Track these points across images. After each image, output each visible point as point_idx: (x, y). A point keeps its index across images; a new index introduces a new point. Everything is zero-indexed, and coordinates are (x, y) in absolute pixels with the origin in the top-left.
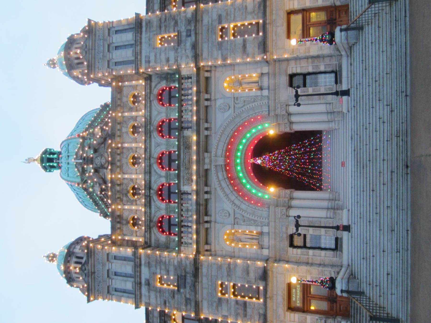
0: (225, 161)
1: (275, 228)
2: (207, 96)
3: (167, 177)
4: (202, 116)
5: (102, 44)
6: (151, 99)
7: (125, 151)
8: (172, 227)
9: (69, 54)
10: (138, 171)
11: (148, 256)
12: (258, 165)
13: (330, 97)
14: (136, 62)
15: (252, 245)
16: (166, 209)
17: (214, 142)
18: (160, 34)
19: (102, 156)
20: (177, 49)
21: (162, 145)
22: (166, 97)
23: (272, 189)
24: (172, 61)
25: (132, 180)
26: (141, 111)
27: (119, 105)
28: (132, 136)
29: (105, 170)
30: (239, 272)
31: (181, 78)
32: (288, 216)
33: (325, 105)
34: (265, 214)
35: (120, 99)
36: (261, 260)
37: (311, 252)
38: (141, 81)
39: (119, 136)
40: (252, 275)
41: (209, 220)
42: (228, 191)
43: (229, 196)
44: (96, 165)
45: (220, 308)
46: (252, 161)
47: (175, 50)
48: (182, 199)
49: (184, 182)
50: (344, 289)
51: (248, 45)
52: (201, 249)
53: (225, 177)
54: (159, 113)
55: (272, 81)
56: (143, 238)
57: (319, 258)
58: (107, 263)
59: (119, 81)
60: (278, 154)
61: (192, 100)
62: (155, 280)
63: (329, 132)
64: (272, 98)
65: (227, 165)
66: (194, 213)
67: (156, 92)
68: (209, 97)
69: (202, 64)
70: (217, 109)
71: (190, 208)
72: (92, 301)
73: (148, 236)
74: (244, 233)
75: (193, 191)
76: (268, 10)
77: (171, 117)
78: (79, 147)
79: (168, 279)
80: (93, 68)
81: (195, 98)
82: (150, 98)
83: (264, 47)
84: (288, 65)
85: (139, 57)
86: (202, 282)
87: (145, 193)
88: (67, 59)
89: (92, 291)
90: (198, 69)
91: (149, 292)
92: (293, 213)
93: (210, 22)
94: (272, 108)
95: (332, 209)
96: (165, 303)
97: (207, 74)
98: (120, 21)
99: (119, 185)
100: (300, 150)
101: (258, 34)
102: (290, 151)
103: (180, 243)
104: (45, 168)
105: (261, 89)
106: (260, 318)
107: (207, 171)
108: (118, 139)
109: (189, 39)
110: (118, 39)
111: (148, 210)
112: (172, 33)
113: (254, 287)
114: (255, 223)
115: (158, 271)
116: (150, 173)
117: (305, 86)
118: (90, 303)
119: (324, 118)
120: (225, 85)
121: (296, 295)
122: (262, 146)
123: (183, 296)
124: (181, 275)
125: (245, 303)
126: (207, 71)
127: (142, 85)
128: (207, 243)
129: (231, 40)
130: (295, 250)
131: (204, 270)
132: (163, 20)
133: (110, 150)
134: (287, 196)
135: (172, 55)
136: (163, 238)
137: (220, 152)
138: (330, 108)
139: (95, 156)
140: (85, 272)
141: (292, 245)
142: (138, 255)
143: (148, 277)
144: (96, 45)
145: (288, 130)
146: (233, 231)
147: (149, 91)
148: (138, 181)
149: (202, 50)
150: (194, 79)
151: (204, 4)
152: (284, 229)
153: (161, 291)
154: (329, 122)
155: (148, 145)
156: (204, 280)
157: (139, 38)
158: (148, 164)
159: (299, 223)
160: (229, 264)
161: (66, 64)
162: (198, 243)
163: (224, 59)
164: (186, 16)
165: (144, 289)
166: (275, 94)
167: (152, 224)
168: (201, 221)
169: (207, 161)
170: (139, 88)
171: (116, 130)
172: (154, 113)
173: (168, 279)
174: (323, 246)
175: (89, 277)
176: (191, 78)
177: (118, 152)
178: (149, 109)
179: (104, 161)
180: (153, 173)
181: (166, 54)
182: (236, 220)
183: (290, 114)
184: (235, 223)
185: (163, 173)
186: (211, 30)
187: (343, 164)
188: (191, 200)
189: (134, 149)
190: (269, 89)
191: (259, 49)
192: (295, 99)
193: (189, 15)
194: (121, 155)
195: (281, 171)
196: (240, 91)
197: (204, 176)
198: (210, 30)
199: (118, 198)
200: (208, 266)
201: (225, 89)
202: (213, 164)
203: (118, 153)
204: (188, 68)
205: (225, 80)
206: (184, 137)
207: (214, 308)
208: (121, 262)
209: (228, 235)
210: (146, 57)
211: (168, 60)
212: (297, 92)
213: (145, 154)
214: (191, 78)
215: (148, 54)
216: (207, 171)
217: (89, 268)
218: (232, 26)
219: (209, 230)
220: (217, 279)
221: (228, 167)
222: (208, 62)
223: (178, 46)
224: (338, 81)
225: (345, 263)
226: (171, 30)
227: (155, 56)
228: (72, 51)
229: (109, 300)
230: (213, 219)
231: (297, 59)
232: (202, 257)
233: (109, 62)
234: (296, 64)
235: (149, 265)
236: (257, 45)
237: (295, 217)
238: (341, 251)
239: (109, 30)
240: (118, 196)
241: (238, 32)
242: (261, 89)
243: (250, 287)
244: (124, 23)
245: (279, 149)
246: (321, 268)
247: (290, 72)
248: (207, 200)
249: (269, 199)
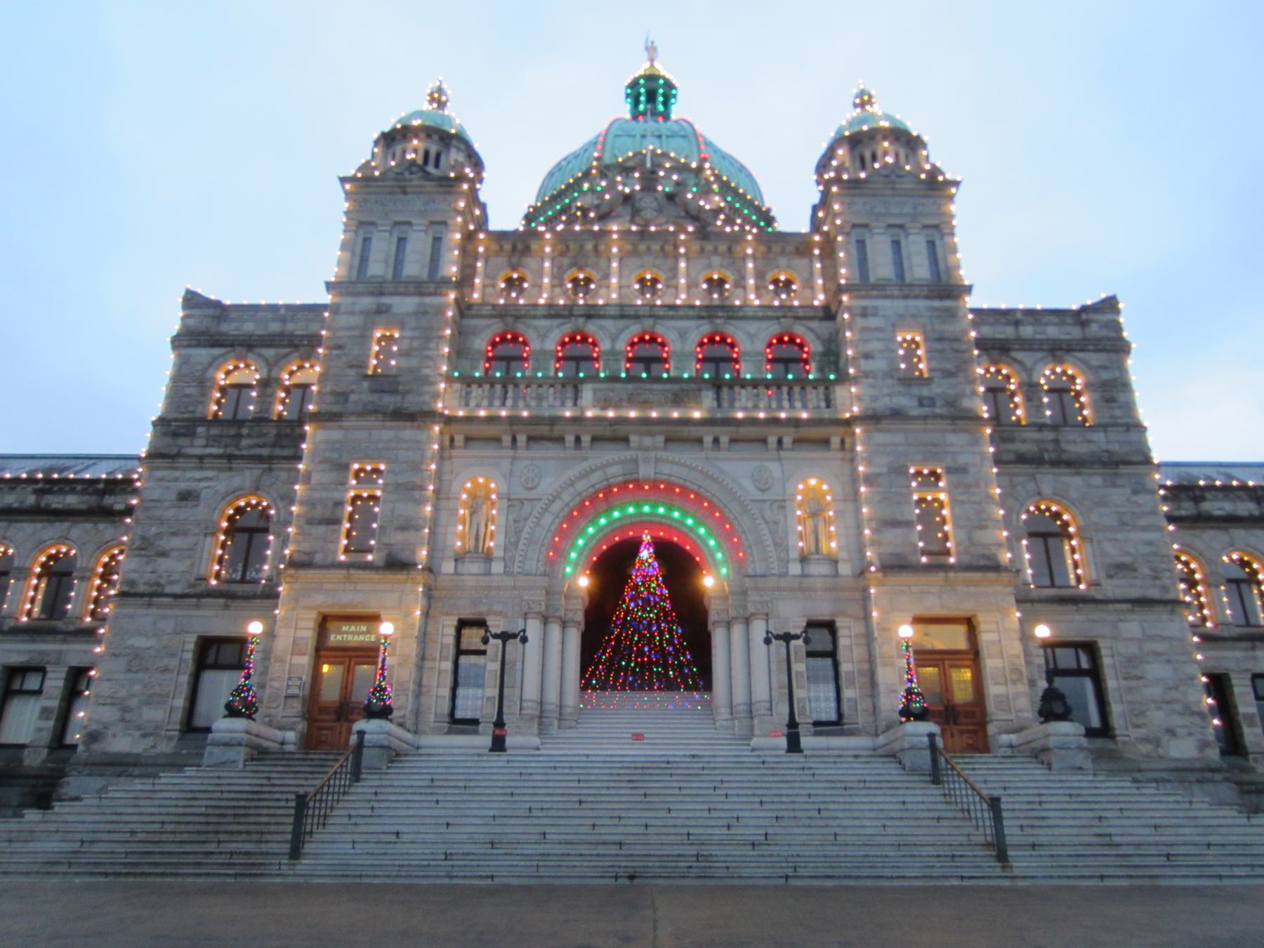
0: (647, 481)
1: (499, 588)
2: (787, 441)
3: (613, 353)
4: (745, 431)
5: (906, 210)
7: (670, 261)
8: (504, 364)
9: (885, 138)
10: (625, 291)
11: (441, 310)
12: (636, 552)
13: (786, 710)
14: (863, 285)
15: (462, 537)
17: (688, 456)
18: (926, 339)
19: (660, 211)
20: (892, 377)
21: (683, 343)
22: (786, 352)
23: (584, 582)
24: (866, 365)
25: (607, 276)
26: (758, 297)
27: (769, 249)
28: (701, 279)
29: (628, 218)
30: (404, 509)
31: (827, 385)
32: (525, 617)
34: (531, 566)
35: (783, 252)
36: (430, 556)
37: (448, 665)
38: (821, 297)
39: (702, 251)
40: (397, 538)
42: (581, 486)
43: (571, 490)
45: (326, 466)
46: (647, 538)
47: (892, 372)
48: (564, 386)
49: (600, 390)
50: (367, 737)
51: (898, 531)
53: (612, 480)
54: (752, 337)
55: (819, 583)
56: (479, 301)
57: (435, 684)
58: (425, 221)
59: (822, 249)
60: (662, 594)
61: (780, 408)
62: (388, 326)
63: (709, 705)
64: (783, 583)
65: (639, 484)
66: (534, 413)
67: (799, 329)
68: (785, 446)
69: (858, 431)
70: (758, 463)
71: (545, 404)
72: (343, 188)
73: (484, 312)
74: (490, 520)
75: (583, 410)
76: (976, 576)
77: (743, 364)
78: (678, 161)
79: (391, 355)
80: (852, 191)
81: (783, 415)
82: (784, 317)
83: (896, 565)
85: (874, 293)
86: (384, 427)
87: (578, 306)
88: (874, 135)
89: (363, 187)
90: (848, 423)
91: (362, 312)
92: (533, 629)
93: (951, 449)
94: (761, 583)
95: (542, 711)
96: (339, 347)
97: (835, 441)
98: (954, 250)
99: (596, 248)
100: (670, 642)
101: (924, 552)
102: (666, 621)
103: (467, 381)
104: (634, 85)
105: (804, 559)
106: (305, 553)
107: (625, 440)
108: (696, 247)
109: (915, 403)
110: (915, 247)
111: (540, 312)
112: (928, 365)
113: (373, 542)
114: (511, 545)
115: (408, 333)
116: (622, 317)
117: (810, 654)
119: (740, 696)
120: (813, 482)
121: (353, 633)
122: (678, 562)
123: (354, 387)
124: (398, 383)
125: (337, 522)
126: (843, 442)
127: (814, 298)
128: (468, 439)
129: (911, 494)
130: (452, 631)
131: (409, 433)
132: (955, 345)
133: (671, 229)
134: (570, 615)
135: (879, 365)
136: (480, 343)
137: (666, 469)
138: (761, 709)
139: (659, 196)
140: (407, 174)
141: (463, 624)
142: (444, 291)
143: (395, 310)
144: (904, 199)
145: (713, 617)
146: (494, 497)
147: (801, 313)
148: (603, 291)
149: (889, 431)
150: (826, 414)
151: (991, 435)
152: (497, 607)
153: (365, 338)
155: (681, 313)
156: (387, 433)
157: (916, 292)
158: (641, 313)
159: (511, 641)
160: (423, 488)
161: (861, 133)
162: (469, 420)
163: (869, 480)
164: (964, 395)
165: (367, 302)
166: (791, 589)
167: (510, 320)
168: (515, 428)
169: (647, 441)
170: (807, 293)
172: (752, 327)
173: (391, 355)
174: (461, 692)
175: (396, 180)
176: (828, 406)
177: (669, 248)
178: (761, 314)
180: (621, 323)
181: (881, 351)
182: (517, 503)
183: (747, 621)
184: (512, 502)
185: (622, 345)
186: (932, 452)
187: (638, 737)
188: (563, 405)
189: (673, 282)
190: (803, 576)
191: (891, 554)
192: (781, 633)
193: (966, 403)
195: (624, 602)
196: (799, 513)
197: (613, 435)
198: (933, 449)
199: (568, 247)
200: (418, 442)
201: (804, 480)
202: (640, 454)
204: (851, 400)
205: (822, 480)
206: (700, 390)
207: (328, 454)
208: (429, 250)
209: (486, 486)
210: (875, 308)
211: (867, 356)
212: (796, 637)
213: (662, 306)
215: (881, 313)
216: (625, 440)
217: (416, 180)
218: (942, 496)
220: (388, 461)
221: (632, 487)
222: (863, 444)
223: (900, 379)
224: (820, 726)
225: (425, 740)
226: (934, 364)
227: (878, 329)
228: (891, 143)
229: (346, 224)
230: (521, 453)
231: (868, 638)
232: (437, 429)
233: (866, 226)
234: (856, 636)
235: (421, 313)
236: (898, 550)
237: (524, 631)
238: (450, 732)
239: (936, 227)
240: (572, 246)
241: (930, 512)
242: (804, 559)
243: (372, 534)
244: (951, 260)
245: (671, 597)
246: (411, 686)
247: (840, 623)
248: (560, 440)
249: (564, 575)
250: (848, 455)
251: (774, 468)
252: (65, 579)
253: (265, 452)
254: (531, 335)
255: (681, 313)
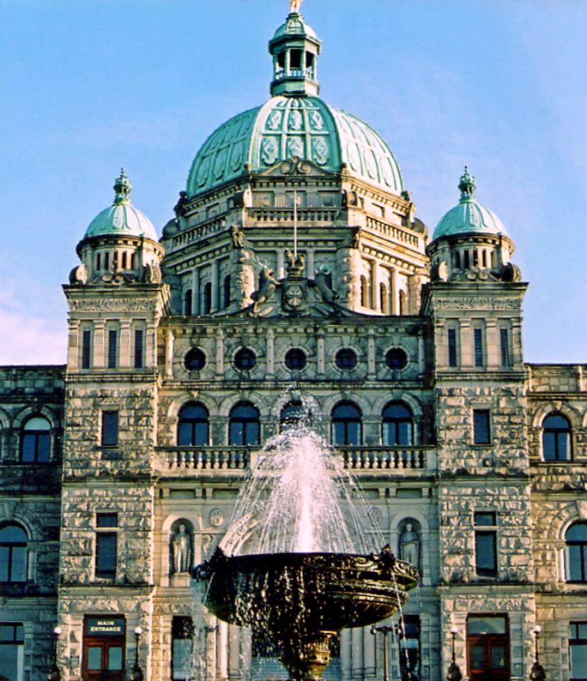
2: (392, 492)
6: (394, 391)
7: (311, 340)
16: (219, 418)
25: (264, 355)
33: (373, 666)
39: (336, 330)
41: (207, 495)
44: (289, 287)
52: (164, 485)
54: (372, 406)
67: (406, 398)
68: (391, 494)
82: (396, 388)
84: (433, 615)
85: (459, 378)
99: (255, 330)
116: (276, 389)
118: (62, 289)
119: (357, 664)
126: (430, 491)
128: (172, 490)
154: (351, 670)
155: (320, 386)
167: (195, 394)
168: (205, 484)
171: (345, 326)
172: (372, 395)
176: (421, 466)
179: (295, 303)
180: (275, 393)
194: (305, 335)
199: (234, 330)
203: (309, 331)
214: (421, 466)
219: (190, 494)
230: (209, 501)
250: (434, 501)
251: (383, 508)
252: (19, 628)
253: (17, 487)
254: (210, 404)
255: (320, 386)
